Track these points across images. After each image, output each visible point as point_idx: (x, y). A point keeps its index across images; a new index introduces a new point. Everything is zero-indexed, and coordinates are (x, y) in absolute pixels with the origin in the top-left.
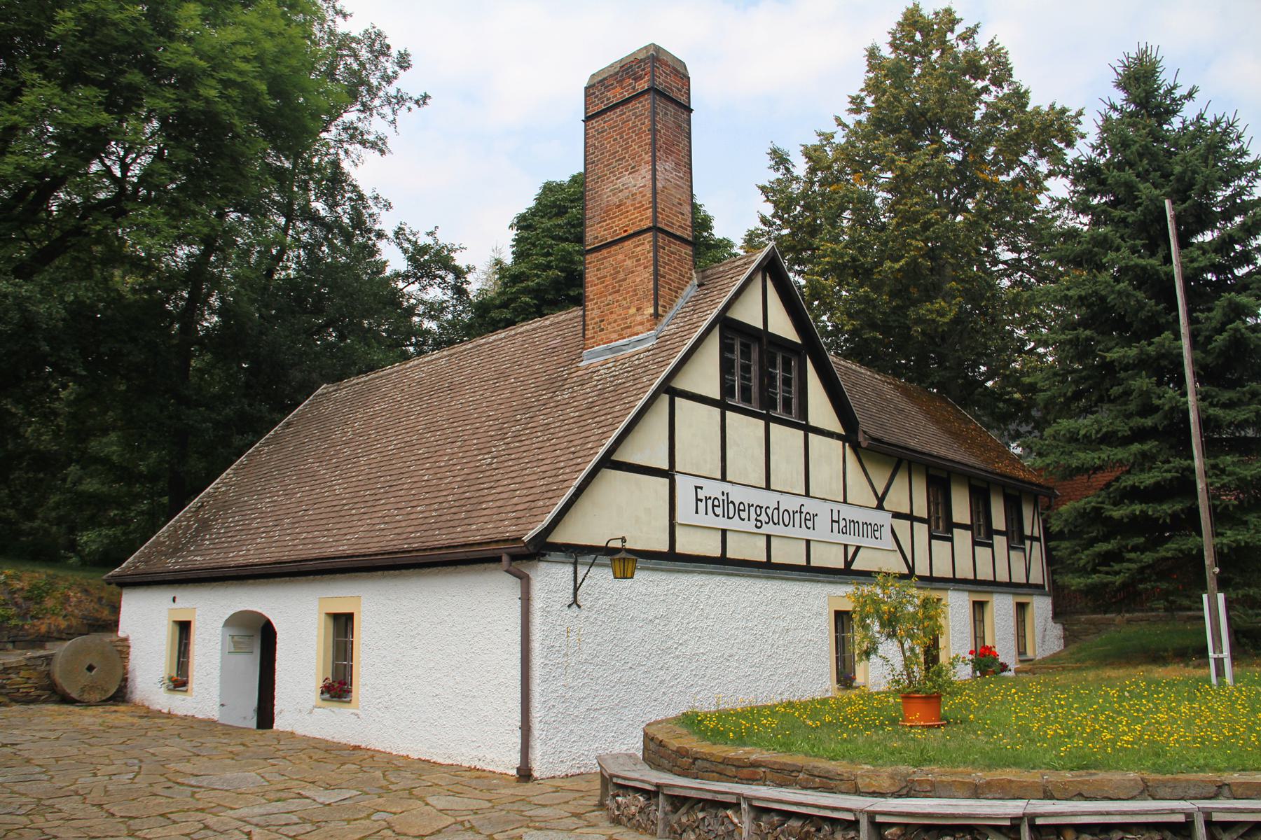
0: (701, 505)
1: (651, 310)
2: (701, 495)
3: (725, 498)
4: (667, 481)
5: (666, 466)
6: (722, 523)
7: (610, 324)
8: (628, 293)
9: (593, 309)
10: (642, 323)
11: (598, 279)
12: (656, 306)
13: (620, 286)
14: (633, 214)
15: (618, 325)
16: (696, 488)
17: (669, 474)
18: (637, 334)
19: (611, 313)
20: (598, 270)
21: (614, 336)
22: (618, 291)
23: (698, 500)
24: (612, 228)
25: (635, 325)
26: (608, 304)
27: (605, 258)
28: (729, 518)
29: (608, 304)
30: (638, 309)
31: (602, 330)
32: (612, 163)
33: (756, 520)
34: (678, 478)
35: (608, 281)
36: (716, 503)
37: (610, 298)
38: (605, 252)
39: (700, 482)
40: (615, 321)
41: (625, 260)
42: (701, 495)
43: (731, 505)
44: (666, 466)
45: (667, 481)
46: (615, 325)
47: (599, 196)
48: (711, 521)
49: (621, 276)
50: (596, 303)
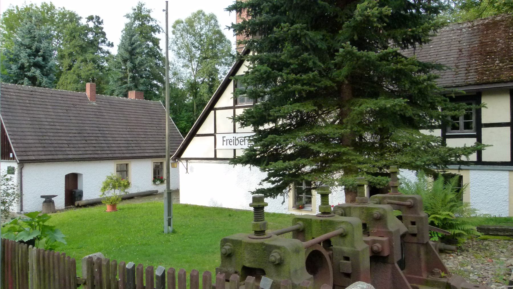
0: (225, 143)
2: (225, 139)
3: (234, 138)
4: (213, 137)
5: (213, 132)
6: (235, 147)
16: (223, 137)
17: (214, 135)
23: (223, 141)
28: (236, 145)
33: (248, 144)
34: (217, 135)
36: (231, 141)
39: (224, 135)
42: (225, 139)
43: (237, 141)
44: (213, 132)
45: (213, 137)
48: (229, 147)
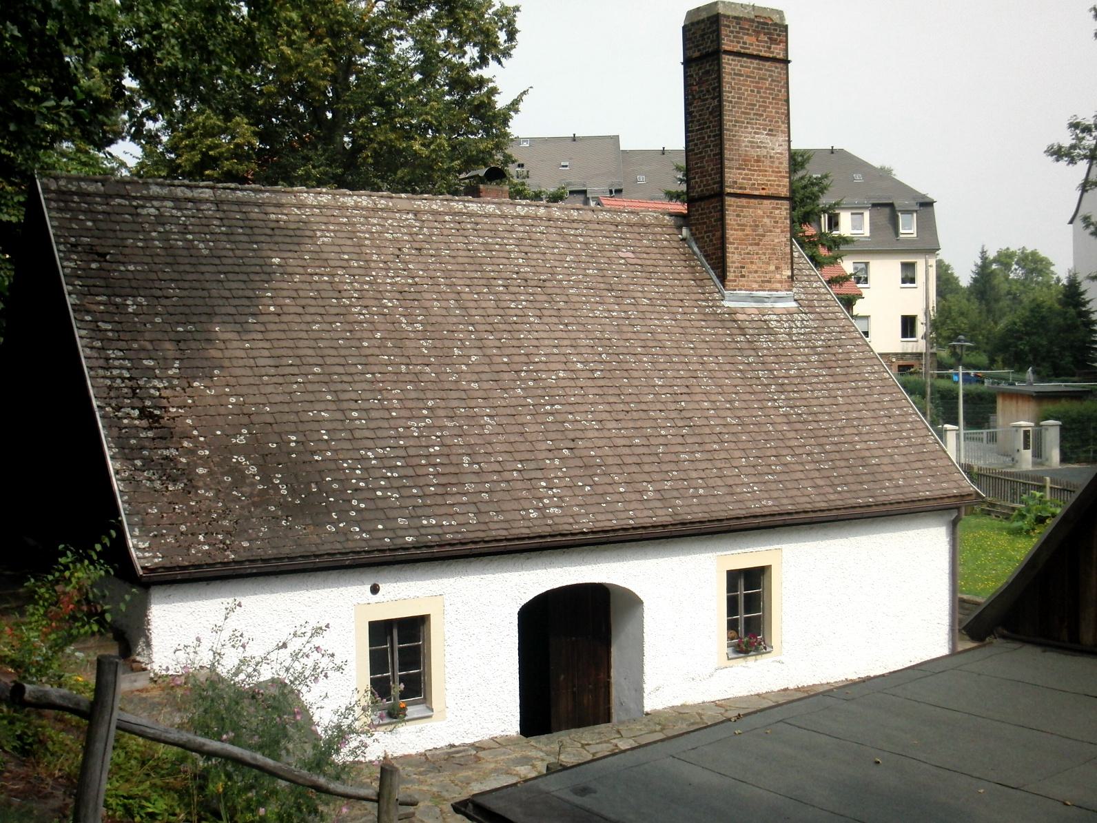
1: (789, 273)
7: (750, 272)
8: (767, 249)
9: (733, 253)
10: (781, 282)
11: (739, 225)
12: (792, 269)
13: (761, 240)
14: (771, 176)
15: (759, 277)
18: (777, 291)
19: (752, 263)
20: (738, 216)
21: (755, 286)
22: (758, 244)
24: (750, 179)
25: (775, 282)
26: (748, 254)
27: (743, 207)
29: (748, 254)
30: (777, 268)
31: (743, 276)
32: (749, 114)
35: (748, 231)
37: (750, 248)
38: (744, 201)
40: (756, 272)
41: (763, 217)
46: (756, 275)
47: (737, 141)
49: (760, 231)
50: (737, 248)
